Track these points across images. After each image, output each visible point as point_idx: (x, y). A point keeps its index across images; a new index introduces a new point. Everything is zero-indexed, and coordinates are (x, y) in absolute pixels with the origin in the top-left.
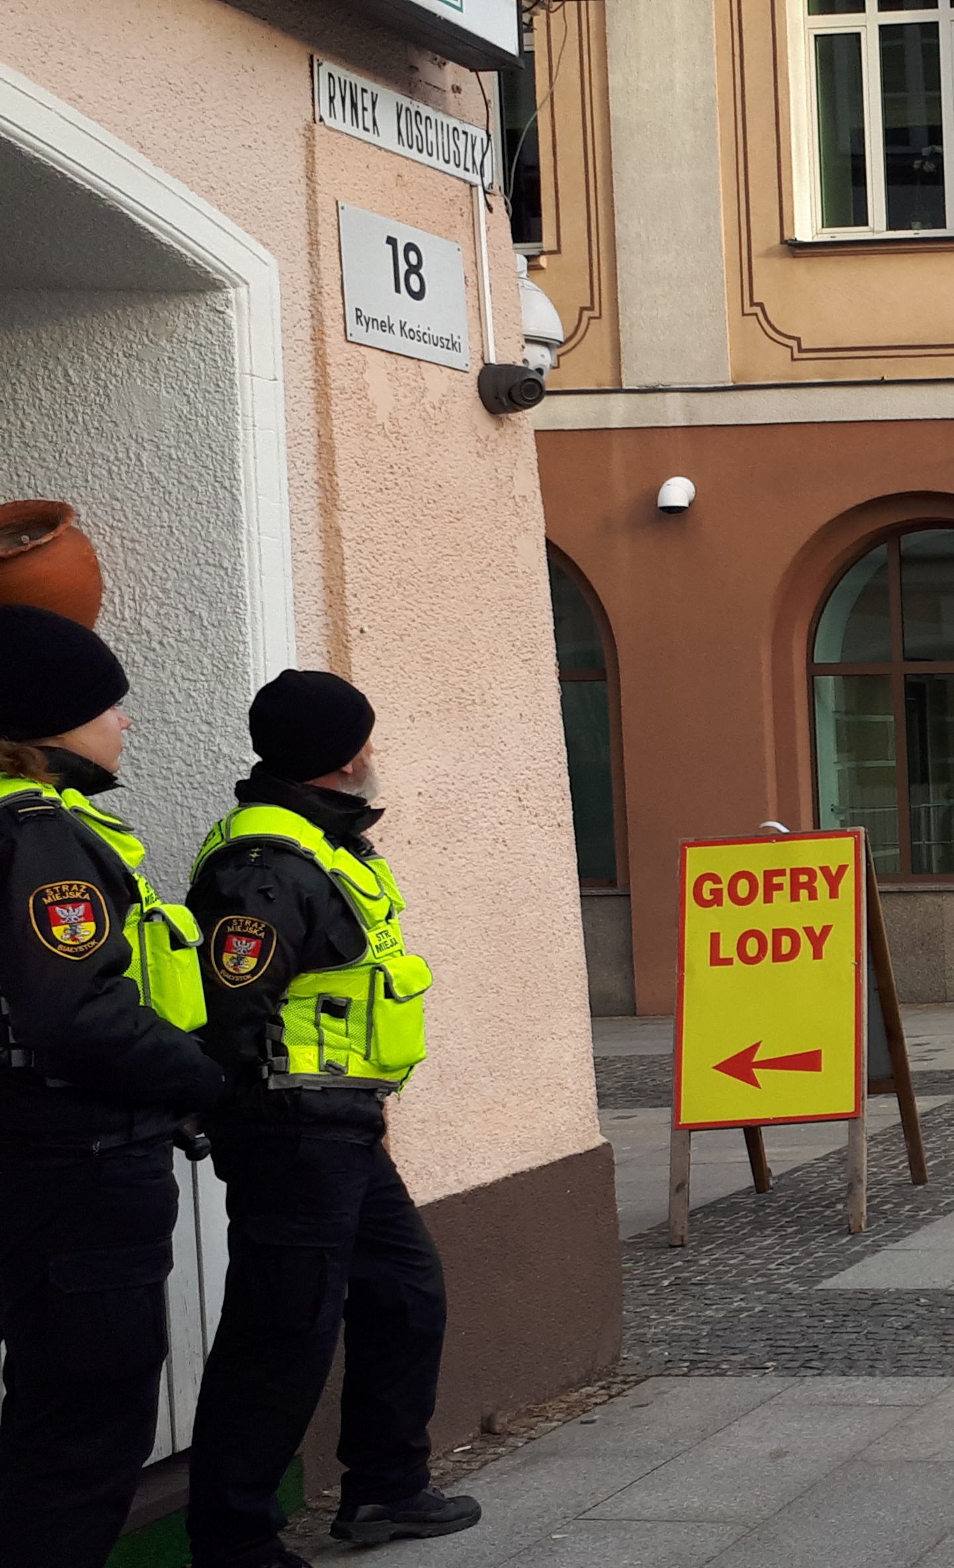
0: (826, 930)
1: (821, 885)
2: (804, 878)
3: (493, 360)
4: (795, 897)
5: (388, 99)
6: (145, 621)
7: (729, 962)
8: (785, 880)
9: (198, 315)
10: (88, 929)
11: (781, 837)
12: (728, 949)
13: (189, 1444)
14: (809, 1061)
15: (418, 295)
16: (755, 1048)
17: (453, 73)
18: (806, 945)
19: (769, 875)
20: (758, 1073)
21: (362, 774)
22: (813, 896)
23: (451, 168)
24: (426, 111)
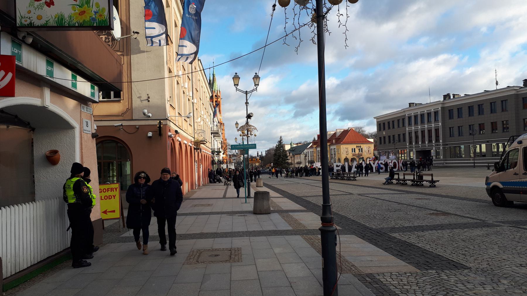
0: (115, 195)
1: (115, 190)
2: (112, 189)
3: (93, 133)
4: (111, 191)
5: (86, 107)
6: (65, 162)
7: (103, 199)
8: (110, 189)
9: (71, 131)
10: (87, 190)
11: (109, 184)
12: (103, 198)
13: (70, 246)
14: (114, 211)
15: (88, 127)
16: (107, 210)
17: (90, 103)
18: (113, 197)
19: (108, 189)
20: (107, 213)
21: (89, 177)
22: (113, 191)
23: (89, 113)
24: (88, 107)
